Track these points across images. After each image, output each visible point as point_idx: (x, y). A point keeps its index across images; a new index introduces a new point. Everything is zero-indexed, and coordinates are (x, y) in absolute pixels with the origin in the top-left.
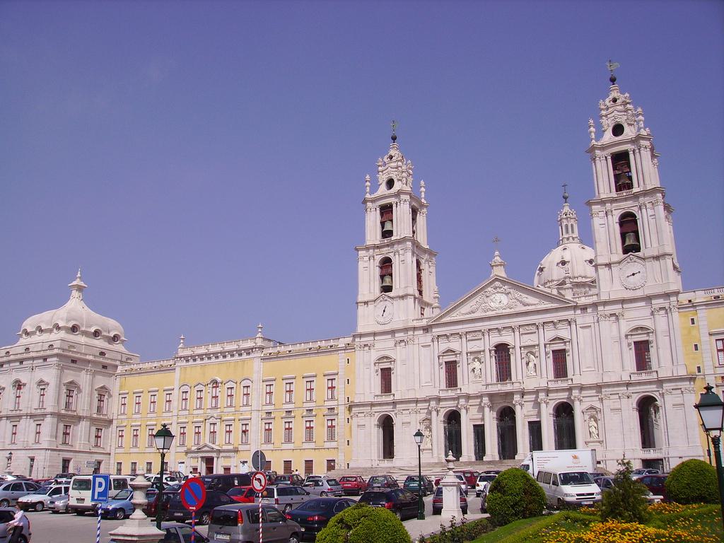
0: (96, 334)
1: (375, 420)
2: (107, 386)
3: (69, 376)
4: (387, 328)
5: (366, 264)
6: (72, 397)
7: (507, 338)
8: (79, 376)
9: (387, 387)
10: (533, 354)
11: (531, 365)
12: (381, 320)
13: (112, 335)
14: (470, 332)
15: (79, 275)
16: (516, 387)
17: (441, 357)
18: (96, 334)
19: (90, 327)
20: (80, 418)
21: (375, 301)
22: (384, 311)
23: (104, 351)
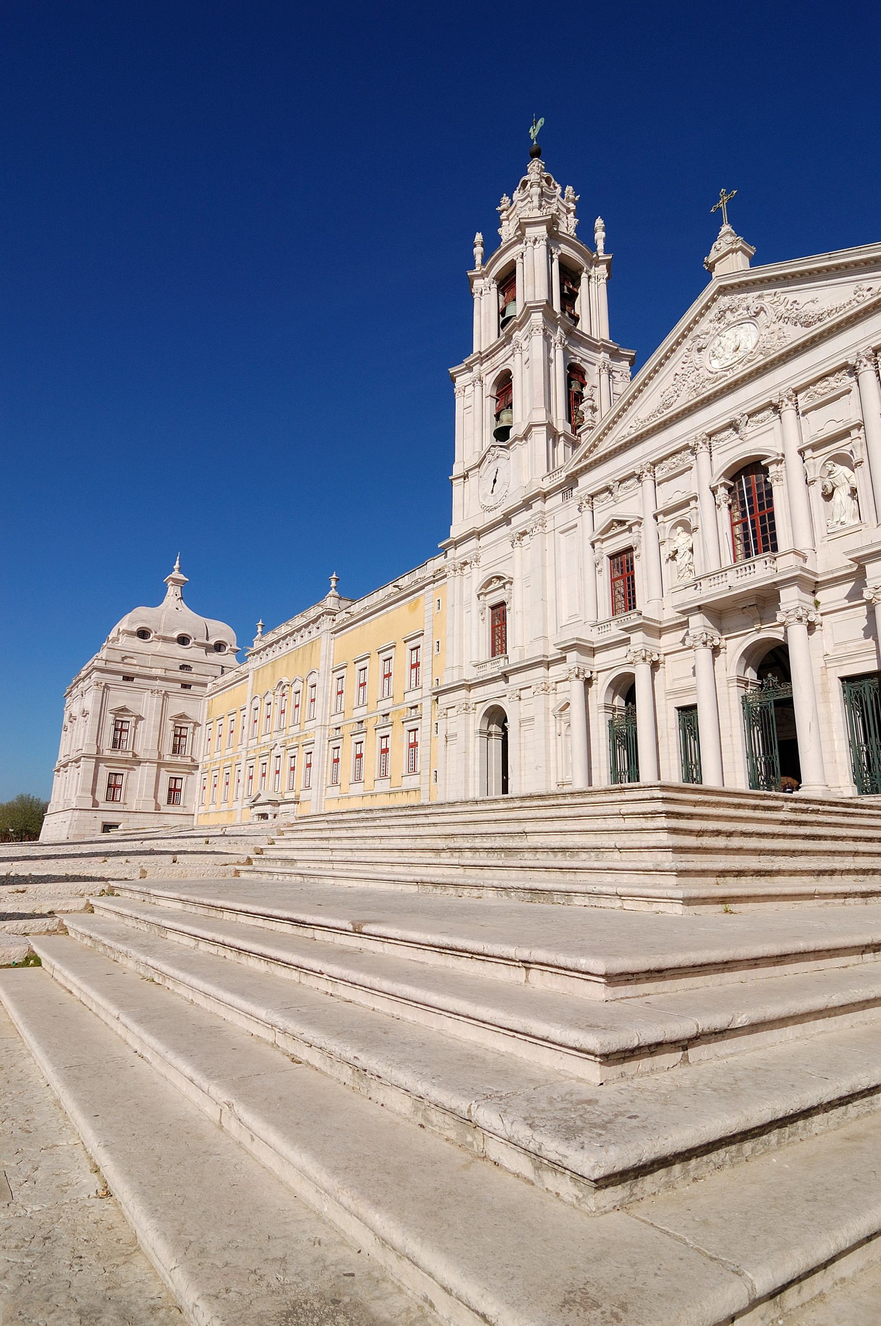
0: (183, 640)
1: (476, 720)
2: (188, 714)
3: (119, 698)
4: (497, 514)
5: (469, 402)
6: (127, 731)
7: (759, 440)
8: (140, 700)
9: (499, 641)
10: (842, 459)
11: (841, 495)
12: (490, 502)
13: (212, 642)
14: (661, 460)
15: (177, 566)
16: (786, 564)
17: (597, 545)
18: (183, 640)
19: (174, 630)
20: (139, 763)
21: (479, 466)
22: (495, 481)
23: (187, 663)
